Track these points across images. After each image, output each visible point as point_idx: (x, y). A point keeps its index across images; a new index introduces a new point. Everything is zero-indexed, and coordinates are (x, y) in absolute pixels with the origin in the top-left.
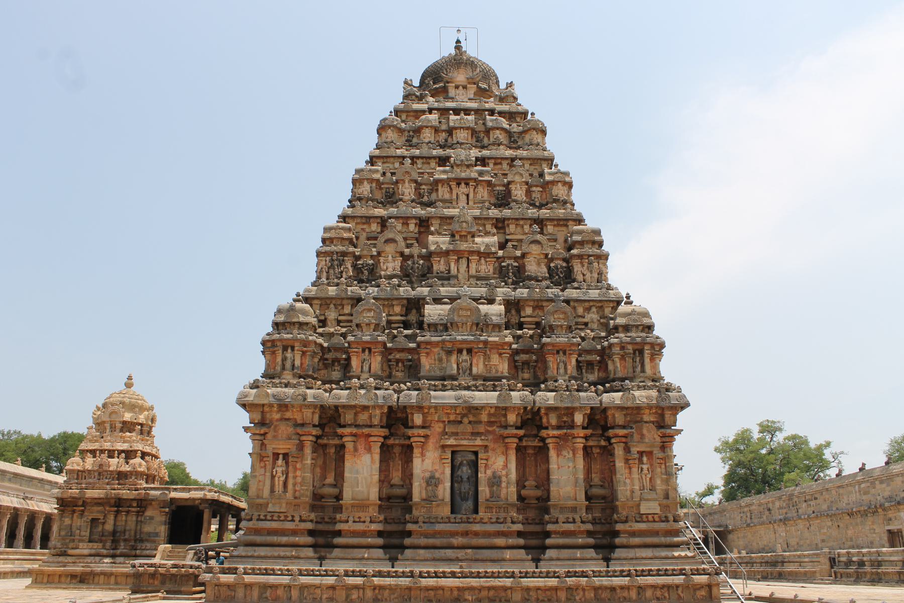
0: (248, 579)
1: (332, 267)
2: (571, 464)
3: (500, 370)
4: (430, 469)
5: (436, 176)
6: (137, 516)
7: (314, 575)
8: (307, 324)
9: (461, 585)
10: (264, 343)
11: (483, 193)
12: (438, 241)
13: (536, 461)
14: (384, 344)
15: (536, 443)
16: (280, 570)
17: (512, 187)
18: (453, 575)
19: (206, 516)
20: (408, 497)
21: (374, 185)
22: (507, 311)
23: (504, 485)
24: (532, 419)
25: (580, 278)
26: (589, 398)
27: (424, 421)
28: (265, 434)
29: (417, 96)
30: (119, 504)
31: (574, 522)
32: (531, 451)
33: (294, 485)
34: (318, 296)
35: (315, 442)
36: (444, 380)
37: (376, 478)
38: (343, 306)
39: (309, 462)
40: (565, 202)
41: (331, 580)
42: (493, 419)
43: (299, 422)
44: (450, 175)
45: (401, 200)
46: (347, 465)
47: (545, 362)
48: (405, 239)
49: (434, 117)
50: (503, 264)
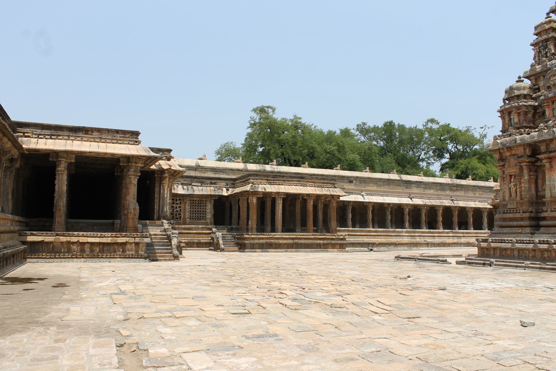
0: (493, 245)
1: (540, 52)
8: (520, 95)
10: (501, 112)
28: (504, 165)
33: (521, 192)
34: (531, 74)
39: (526, 177)
41: (531, 246)
43: (519, 155)
46: (547, 177)
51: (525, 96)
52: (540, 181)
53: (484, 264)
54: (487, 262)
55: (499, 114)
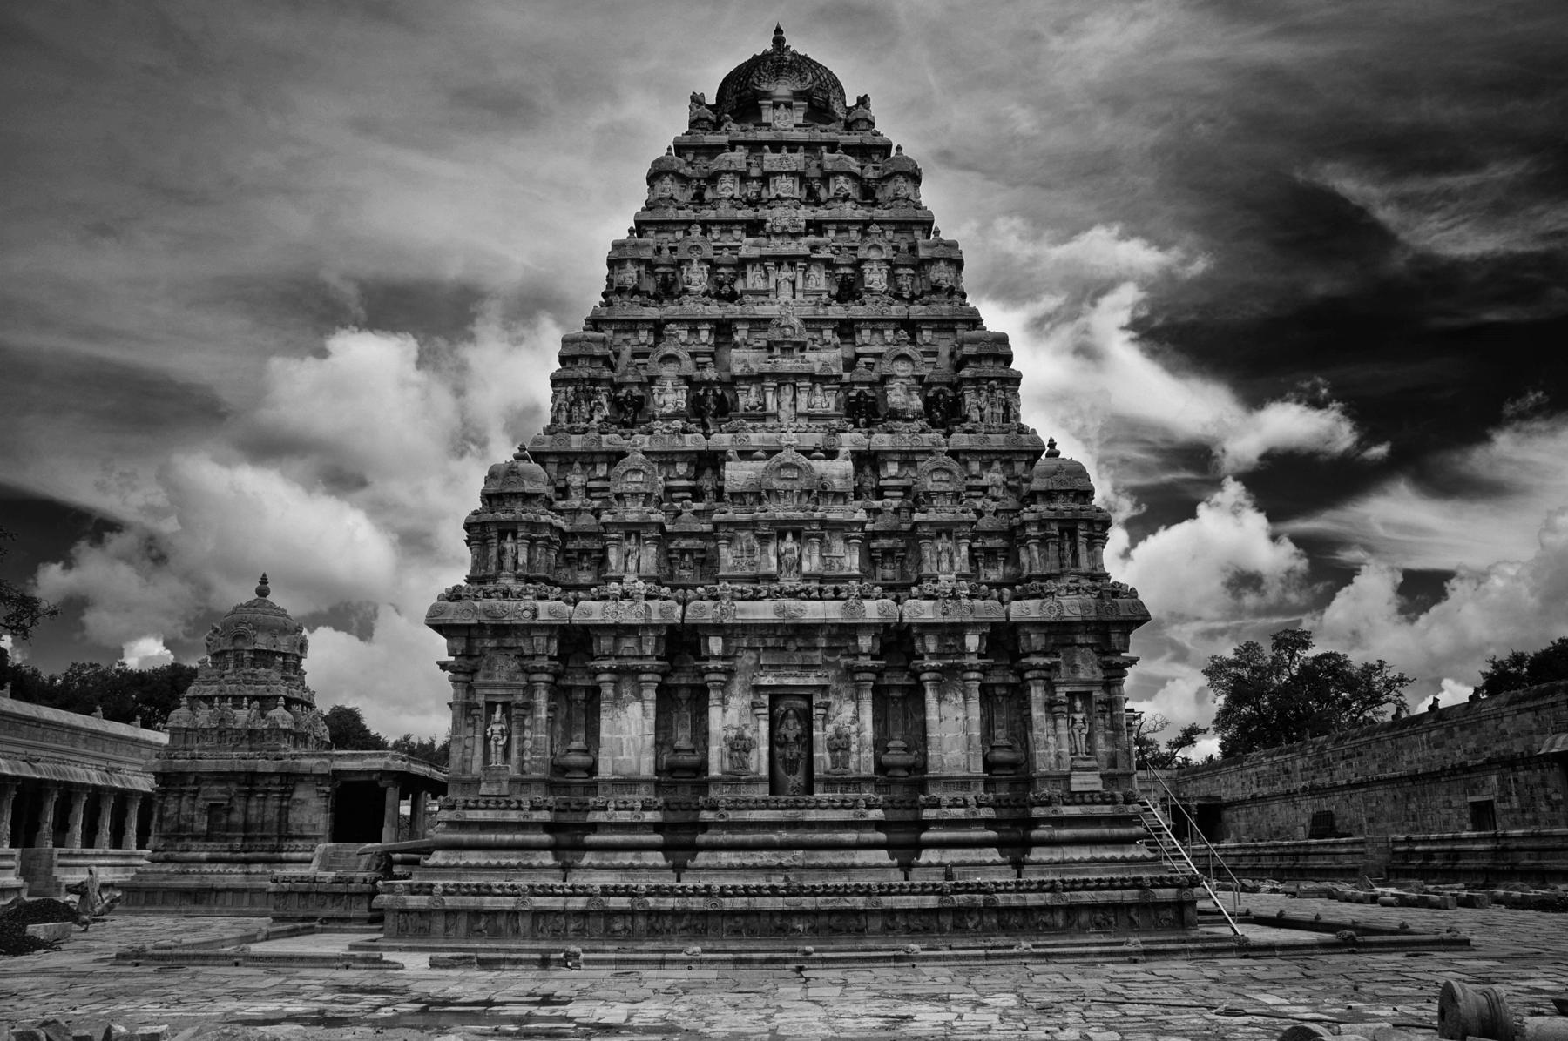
0: (450, 902)
1: (576, 403)
3: (847, 564)
4: (736, 723)
5: (743, 253)
6: (282, 799)
7: (554, 895)
9: (786, 908)
11: (819, 279)
12: (743, 359)
13: (905, 709)
14: (661, 526)
15: (904, 680)
16: (500, 886)
17: (866, 268)
19: (391, 795)
20: (702, 767)
21: (643, 268)
22: (858, 468)
23: (854, 748)
24: (897, 641)
25: (975, 415)
26: (989, 610)
27: (726, 647)
28: (473, 672)
29: (710, 122)
30: (250, 781)
31: (965, 805)
32: (896, 694)
33: (521, 752)
35: (554, 684)
36: (758, 584)
37: (650, 739)
38: (594, 465)
39: (543, 715)
40: (951, 291)
41: (579, 903)
43: (527, 652)
44: (768, 251)
45: (686, 291)
46: (605, 720)
47: (919, 551)
48: (693, 355)
49: (738, 157)
50: (853, 394)
54: (553, 956)
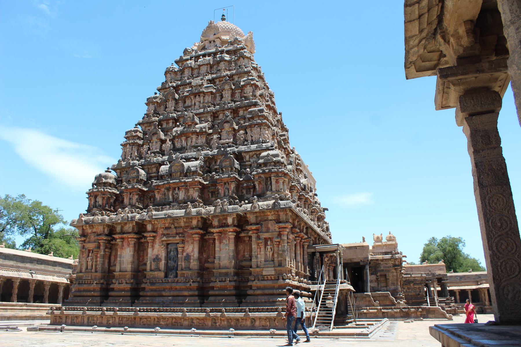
2: (227, 248)
4: (156, 254)
18: (155, 311)
20: (145, 270)
23: (192, 261)
33: (96, 265)
42: (186, 225)
51: (110, 185)
52: (113, 258)
53: (55, 330)
55: (87, 196)
